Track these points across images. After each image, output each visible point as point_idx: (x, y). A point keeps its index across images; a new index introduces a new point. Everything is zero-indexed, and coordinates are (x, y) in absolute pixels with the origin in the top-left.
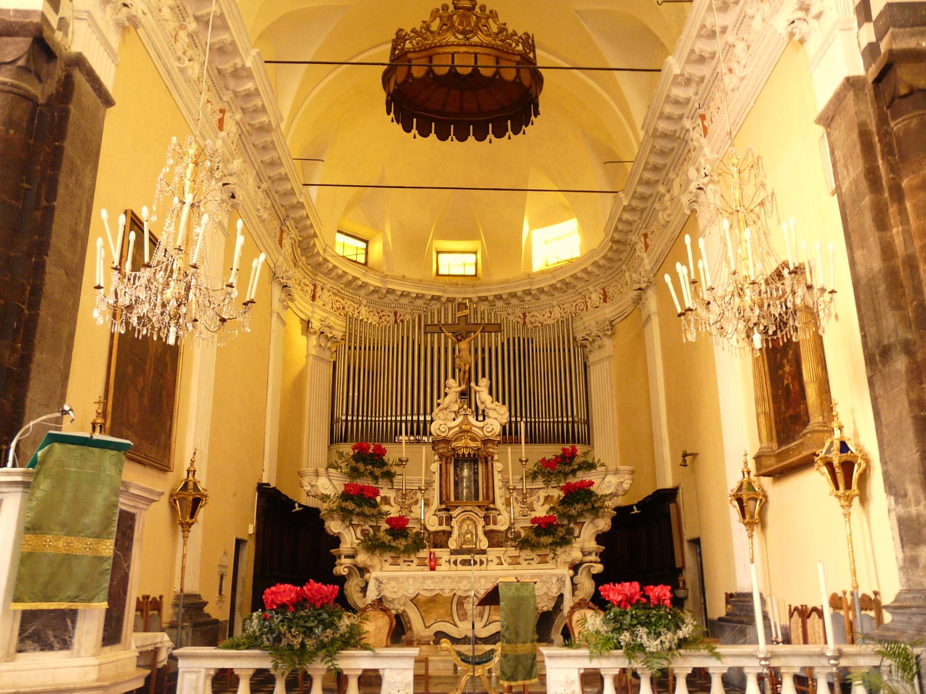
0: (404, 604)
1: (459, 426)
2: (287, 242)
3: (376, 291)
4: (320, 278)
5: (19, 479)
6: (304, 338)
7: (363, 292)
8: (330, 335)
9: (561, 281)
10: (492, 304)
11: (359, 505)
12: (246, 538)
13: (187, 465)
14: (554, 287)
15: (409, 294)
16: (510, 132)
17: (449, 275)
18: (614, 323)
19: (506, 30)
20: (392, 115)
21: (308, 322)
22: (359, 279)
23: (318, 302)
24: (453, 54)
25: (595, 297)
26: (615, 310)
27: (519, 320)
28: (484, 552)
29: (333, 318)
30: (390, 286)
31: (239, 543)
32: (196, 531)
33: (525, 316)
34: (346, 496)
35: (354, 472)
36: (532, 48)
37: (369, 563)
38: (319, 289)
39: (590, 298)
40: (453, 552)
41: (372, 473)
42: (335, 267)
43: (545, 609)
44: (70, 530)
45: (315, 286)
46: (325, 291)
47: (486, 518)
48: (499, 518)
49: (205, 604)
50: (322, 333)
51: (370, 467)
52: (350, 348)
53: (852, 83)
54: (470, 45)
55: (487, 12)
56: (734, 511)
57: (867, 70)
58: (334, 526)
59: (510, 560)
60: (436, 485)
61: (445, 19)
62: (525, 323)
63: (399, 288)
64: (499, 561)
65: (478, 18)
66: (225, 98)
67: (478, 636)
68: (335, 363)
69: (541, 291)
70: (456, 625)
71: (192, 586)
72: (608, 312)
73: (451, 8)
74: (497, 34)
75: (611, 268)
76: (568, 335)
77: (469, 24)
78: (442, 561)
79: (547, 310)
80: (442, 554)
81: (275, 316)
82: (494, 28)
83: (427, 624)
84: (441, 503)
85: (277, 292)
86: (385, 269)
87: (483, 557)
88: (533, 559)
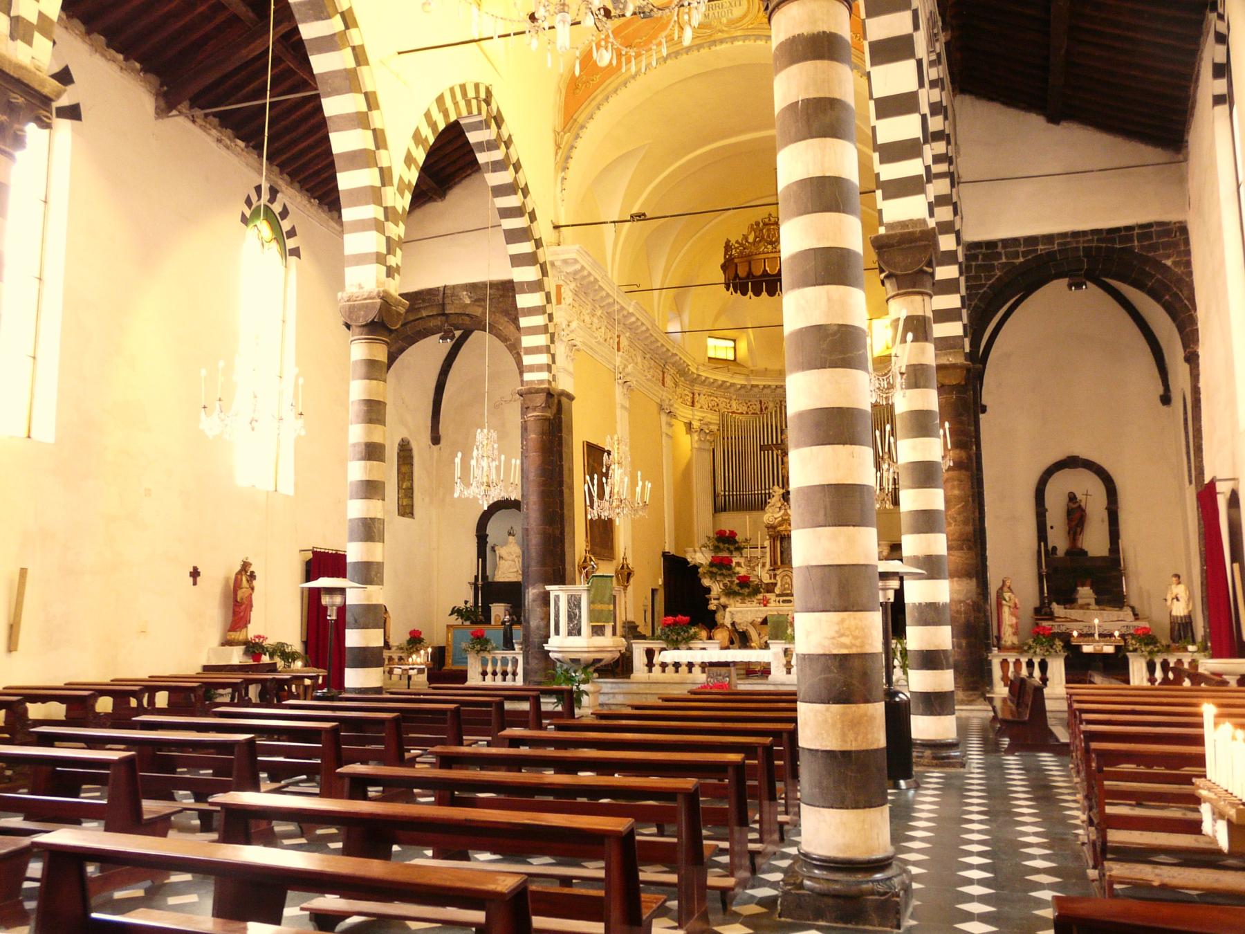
0: (747, 626)
1: (782, 516)
3: (743, 387)
4: (697, 388)
6: (689, 436)
8: (707, 431)
11: (720, 569)
12: (657, 587)
13: (622, 555)
15: (769, 386)
20: (731, 289)
21: (690, 423)
23: (697, 405)
29: (709, 416)
30: (753, 383)
31: (654, 591)
32: (630, 588)
34: (711, 565)
35: (716, 549)
37: (727, 603)
38: (697, 395)
40: (777, 596)
41: (728, 549)
42: (707, 378)
44: (601, 602)
45: (693, 394)
46: (702, 395)
49: (638, 626)
51: (727, 545)
52: (724, 439)
58: (706, 582)
60: (768, 555)
61: (757, 234)
63: (761, 382)
68: (714, 450)
71: (631, 618)
73: (761, 224)
78: (772, 601)
80: (771, 596)
81: (664, 436)
85: (664, 418)
86: (749, 364)
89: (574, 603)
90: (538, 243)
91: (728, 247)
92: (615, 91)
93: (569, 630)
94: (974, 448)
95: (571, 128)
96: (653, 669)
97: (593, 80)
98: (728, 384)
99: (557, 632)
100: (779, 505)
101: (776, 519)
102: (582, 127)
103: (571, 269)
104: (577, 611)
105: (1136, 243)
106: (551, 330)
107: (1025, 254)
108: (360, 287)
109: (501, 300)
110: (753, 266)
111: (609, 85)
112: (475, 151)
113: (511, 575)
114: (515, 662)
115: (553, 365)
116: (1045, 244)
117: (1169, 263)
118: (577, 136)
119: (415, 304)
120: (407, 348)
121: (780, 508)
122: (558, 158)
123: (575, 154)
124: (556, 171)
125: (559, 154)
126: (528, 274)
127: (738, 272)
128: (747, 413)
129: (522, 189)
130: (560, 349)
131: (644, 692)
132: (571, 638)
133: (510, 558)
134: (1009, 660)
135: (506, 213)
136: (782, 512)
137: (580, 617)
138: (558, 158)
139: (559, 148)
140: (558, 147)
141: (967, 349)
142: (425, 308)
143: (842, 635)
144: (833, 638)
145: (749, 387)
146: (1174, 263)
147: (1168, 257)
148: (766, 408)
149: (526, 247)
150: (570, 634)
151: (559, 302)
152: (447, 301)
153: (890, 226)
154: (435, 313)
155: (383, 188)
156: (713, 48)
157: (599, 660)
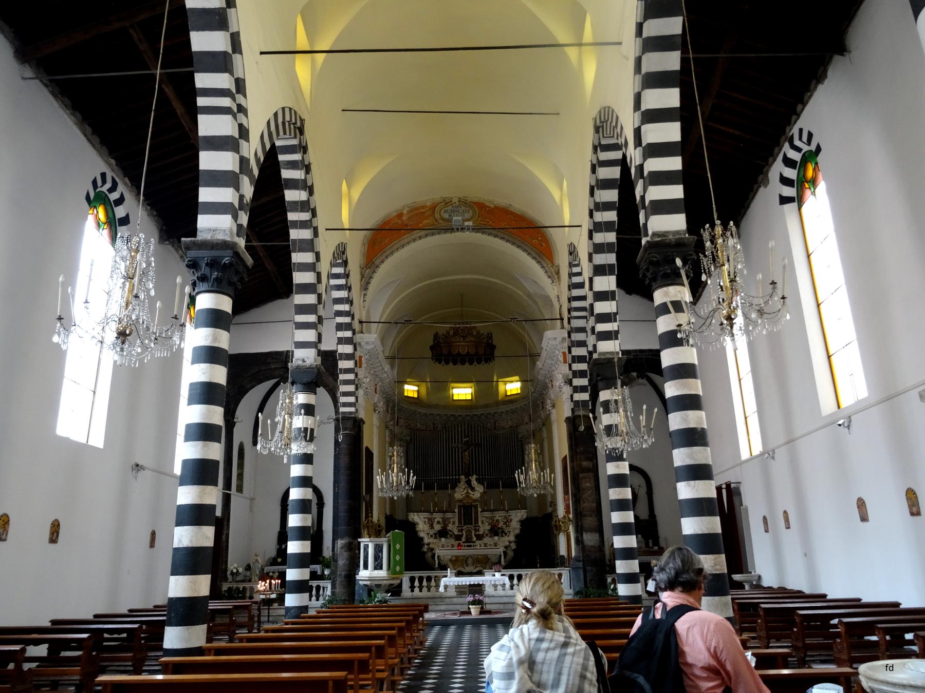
0: (447, 561)
1: (465, 494)
3: (425, 415)
14: (507, 411)
15: (440, 415)
17: (459, 400)
19: (480, 333)
25: (526, 419)
28: (475, 542)
36: (491, 338)
37: (434, 547)
40: (464, 542)
42: (406, 409)
46: (402, 419)
47: (475, 530)
50: (402, 440)
59: (483, 545)
60: (457, 517)
61: (455, 331)
66: (377, 380)
69: (502, 412)
72: (532, 426)
74: (476, 336)
82: (475, 334)
84: (459, 524)
87: (474, 544)
89: (378, 549)
91: (436, 336)
92: (397, 249)
94: (595, 460)
95: (371, 266)
99: (366, 567)
100: (464, 487)
102: (377, 267)
103: (369, 347)
104: (380, 554)
106: (356, 383)
108: (304, 361)
115: (357, 404)
118: (374, 272)
120: (256, 386)
121: (464, 489)
122: (362, 282)
125: (363, 280)
126: (347, 349)
127: (443, 352)
129: (351, 301)
130: (361, 393)
132: (376, 572)
135: (339, 314)
136: (465, 491)
137: (382, 558)
138: (362, 282)
139: (363, 277)
140: (362, 276)
141: (590, 408)
143: (716, 565)
144: (713, 566)
148: (437, 427)
149: (348, 334)
150: (375, 568)
151: (360, 367)
153: (600, 354)
154: (280, 366)
155: (318, 305)
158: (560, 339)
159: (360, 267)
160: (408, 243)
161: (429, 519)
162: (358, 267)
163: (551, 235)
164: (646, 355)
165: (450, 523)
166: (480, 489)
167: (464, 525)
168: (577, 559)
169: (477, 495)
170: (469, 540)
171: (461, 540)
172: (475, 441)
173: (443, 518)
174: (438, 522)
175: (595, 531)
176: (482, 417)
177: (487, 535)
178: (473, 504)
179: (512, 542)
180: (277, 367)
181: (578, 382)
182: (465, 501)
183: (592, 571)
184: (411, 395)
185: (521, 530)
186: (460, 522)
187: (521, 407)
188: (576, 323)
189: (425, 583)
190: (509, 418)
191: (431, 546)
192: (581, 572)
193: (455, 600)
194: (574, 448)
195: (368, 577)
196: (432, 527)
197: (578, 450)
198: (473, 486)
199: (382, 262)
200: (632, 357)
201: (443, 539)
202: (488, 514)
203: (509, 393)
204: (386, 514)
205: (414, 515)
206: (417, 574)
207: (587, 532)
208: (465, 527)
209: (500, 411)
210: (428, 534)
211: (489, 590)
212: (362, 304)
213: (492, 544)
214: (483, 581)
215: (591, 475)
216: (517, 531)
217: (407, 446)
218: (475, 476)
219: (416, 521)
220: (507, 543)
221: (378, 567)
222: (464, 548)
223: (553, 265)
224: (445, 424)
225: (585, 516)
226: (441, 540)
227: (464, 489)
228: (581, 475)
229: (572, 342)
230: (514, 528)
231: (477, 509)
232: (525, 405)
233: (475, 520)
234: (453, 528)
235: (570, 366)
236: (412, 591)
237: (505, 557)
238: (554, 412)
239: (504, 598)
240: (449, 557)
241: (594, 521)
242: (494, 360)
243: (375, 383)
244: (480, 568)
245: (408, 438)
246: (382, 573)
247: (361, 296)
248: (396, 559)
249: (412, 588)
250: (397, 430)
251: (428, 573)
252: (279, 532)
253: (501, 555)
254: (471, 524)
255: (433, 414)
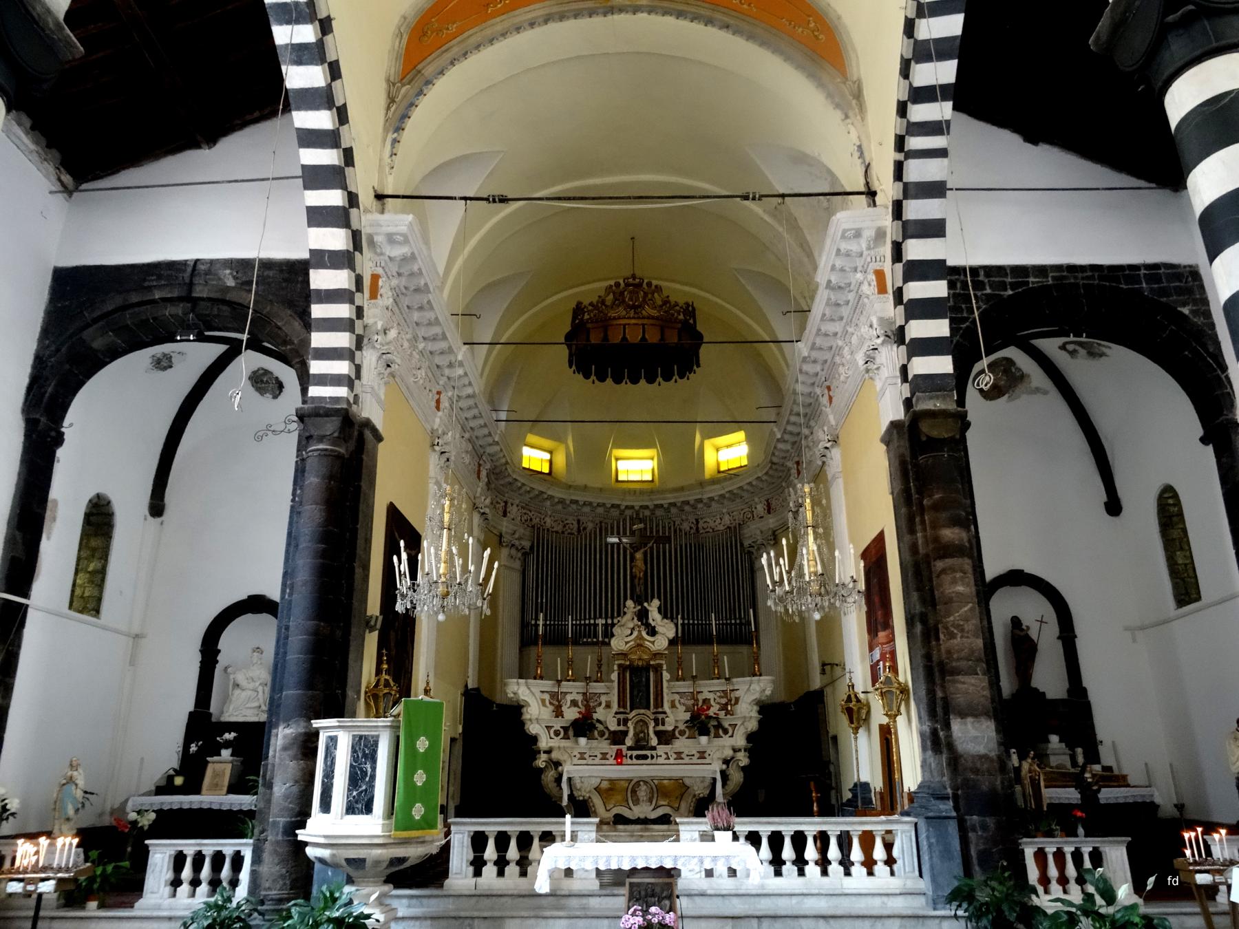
0: (590, 792)
2: (484, 473)
3: (562, 501)
5: (389, 724)
7: (548, 503)
9: (729, 491)
10: (668, 510)
14: (722, 496)
15: (590, 504)
16: (676, 377)
17: (628, 481)
18: (776, 533)
19: (668, 302)
20: (574, 367)
21: (501, 536)
22: (545, 493)
24: (624, 325)
25: (760, 508)
26: (777, 521)
27: (692, 525)
28: (654, 748)
33: (697, 522)
38: (509, 504)
39: (756, 508)
40: (630, 749)
42: (523, 484)
43: (701, 795)
45: (506, 503)
46: (515, 506)
47: (656, 721)
48: (667, 719)
50: (513, 545)
53: (894, 425)
54: (639, 318)
55: (653, 287)
56: (844, 719)
57: (905, 416)
59: (675, 756)
62: (697, 528)
63: (581, 498)
64: (665, 756)
65: (645, 293)
66: (441, 383)
67: (648, 817)
69: (711, 499)
70: (630, 809)
72: (771, 522)
73: (622, 284)
74: (661, 306)
75: (773, 483)
76: (736, 541)
77: (637, 299)
79: (718, 517)
82: (659, 302)
83: (608, 808)
84: (619, 706)
87: (654, 753)
88: (693, 755)
89: (364, 751)
90: (353, 199)
92: (478, 47)
93: (349, 802)
94: (972, 527)
96: (484, 869)
97: (448, 29)
98: (546, 496)
99: (326, 806)
101: (627, 643)
102: (429, 82)
103: (398, 252)
104: (368, 766)
105: (1144, 285)
106: (359, 330)
107: (1014, 286)
109: (284, 285)
110: (610, 333)
111: (468, 37)
112: (271, 19)
113: (249, 712)
114: (238, 860)
115: (357, 382)
116: (1035, 277)
117: (1186, 311)
118: (420, 93)
119: (145, 280)
121: (633, 629)
122: (390, 114)
123: (417, 114)
124: (386, 130)
125: (393, 109)
126: (334, 239)
128: (563, 532)
130: (369, 358)
131: (468, 914)
133: (251, 686)
134: (1047, 850)
136: (635, 633)
137: (373, 777)
138: (390, 114)
140: (391, 100)
142: (159, 287)
145: (568, 502)
146: (1192, 311)
147: (1184, 305)
148: (585, 529)
149: (333, 198)
150: (351, 809)
151: (374, 294)
152: (196, 280)
154: (176, 294)
156: (610, 17)
157: (401, 860)
158: (869, 233)
159: (388, 80)
160: (504, 35)
161: (554, 695)
162: (383, 78)
163: (839, 18)
164: (1083, 278)
165: (600, 704)
166: (667, 630)
167: (631, 710)
168: (929, 791)
169: (660, 643)
170: (641, 744)
171: (623, 743)
172: (658, 531)
173: (584, 694)
174: (574, 703)
175: (986, 714)
176: (674, 510)
177: (682, 733)
178: (652, 663)
179: (740, 750)
180: (169, 296)
181: (921, 329)
182: (633, 657)
183: (984, 827)
184: (536, 467)
185: (760, 722)
186: (621, 703)
187: (750, 484)
188: (918, 171)
189: (513, 853)
190: (725, 511)
191: (554, 755)
192: (953, 828)
193: (594, 902)
194: (915, 496)
195: (325, 837)
196: (558, 713)
197: (925, 502)
198: (653, 624)
199: (442, 73)
200: (1051, 282)
201: (583, 741)
202: (685, 687)
203: (723, 468)
204: (466, 686)
205: (518, 684)
206: (492, 826)
207: (963, 715)
208: (634, 713)
209: (705, 496)
210: (548, 728)
211: (690, 878)
212: (387, 160)
213: (694, 752)
214: (676, 859)
215: (967, 564)
216: (753, 725)
217: (525, 560)
218: (656, 603)
219: (522, 697)
220: (729, 753)
221: (360, 804)
222: (629, 761)
223: (847, 79)
224: (601, 522)
225: (956, 672)
226: (577, 742)
227: (633, 629)
228: (939, 565)
229: (905, 225)
230: (745, 717)
231: (662, 674)
232: (758, 478)
233: (656, 699)
234: (607, 717)
235: (899, 294)
236: (478, 873)
237: (724, 785)
238: (836, 454)
239: (735, 901)
240: (595, 782)
241: (983, 688)
242: (698, 366)
243: (439, 388)
244: (667, 810)
245: (527, 544)
246: (371, 826)
247: (384, 140)
248: (414, 784)
249: (478, 865)
250: (505, 526)
251: (521, 824)
252: (190, 713)
253: (714, 779)
254: (648, 708)
255: (576, 502)
